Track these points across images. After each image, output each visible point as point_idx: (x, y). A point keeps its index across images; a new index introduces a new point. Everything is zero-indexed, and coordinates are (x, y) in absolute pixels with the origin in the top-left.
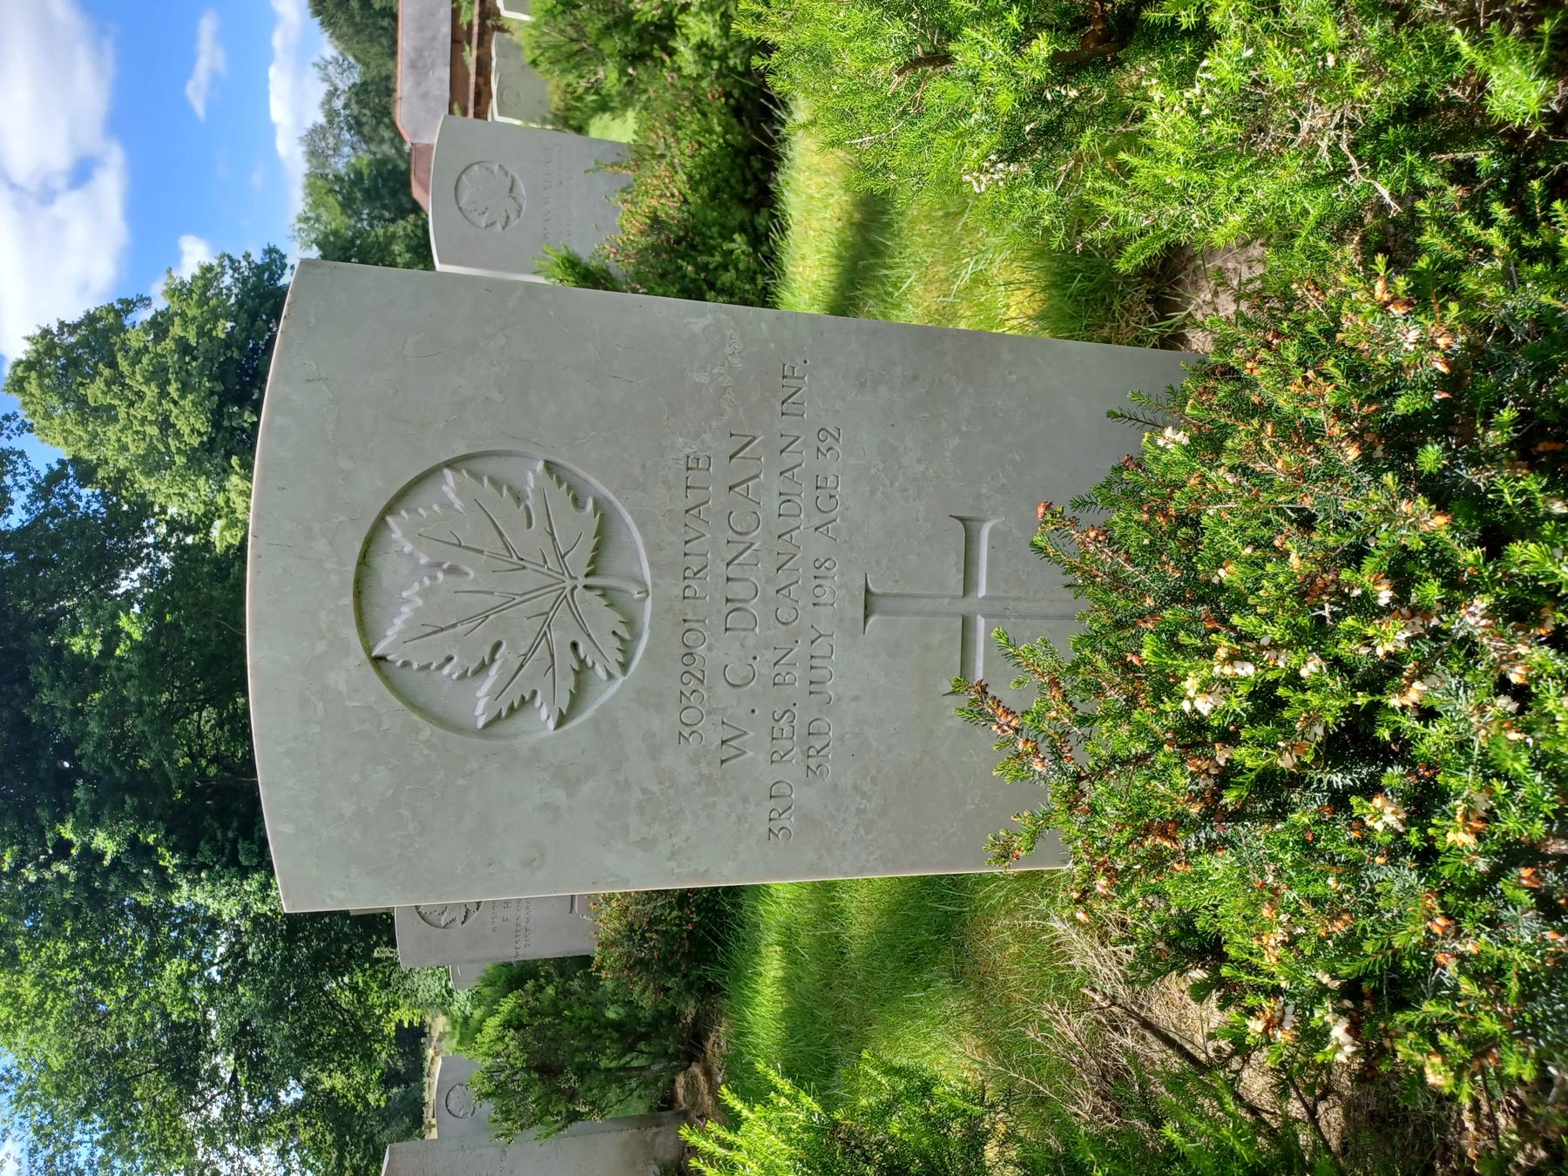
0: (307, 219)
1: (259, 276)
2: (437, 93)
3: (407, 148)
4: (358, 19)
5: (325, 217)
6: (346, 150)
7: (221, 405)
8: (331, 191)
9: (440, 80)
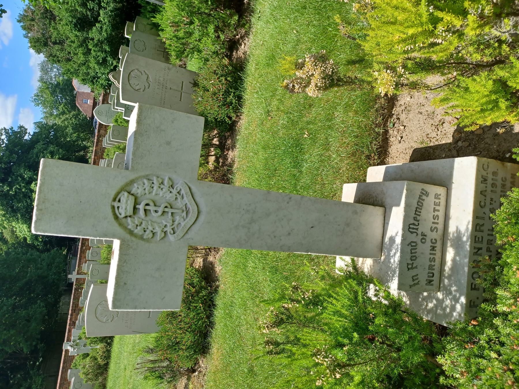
0: (38, 96)
1: (16, 137)
3: (75, 92)
5: (45, 96)
6: (55, 70)
8: (48, 88)
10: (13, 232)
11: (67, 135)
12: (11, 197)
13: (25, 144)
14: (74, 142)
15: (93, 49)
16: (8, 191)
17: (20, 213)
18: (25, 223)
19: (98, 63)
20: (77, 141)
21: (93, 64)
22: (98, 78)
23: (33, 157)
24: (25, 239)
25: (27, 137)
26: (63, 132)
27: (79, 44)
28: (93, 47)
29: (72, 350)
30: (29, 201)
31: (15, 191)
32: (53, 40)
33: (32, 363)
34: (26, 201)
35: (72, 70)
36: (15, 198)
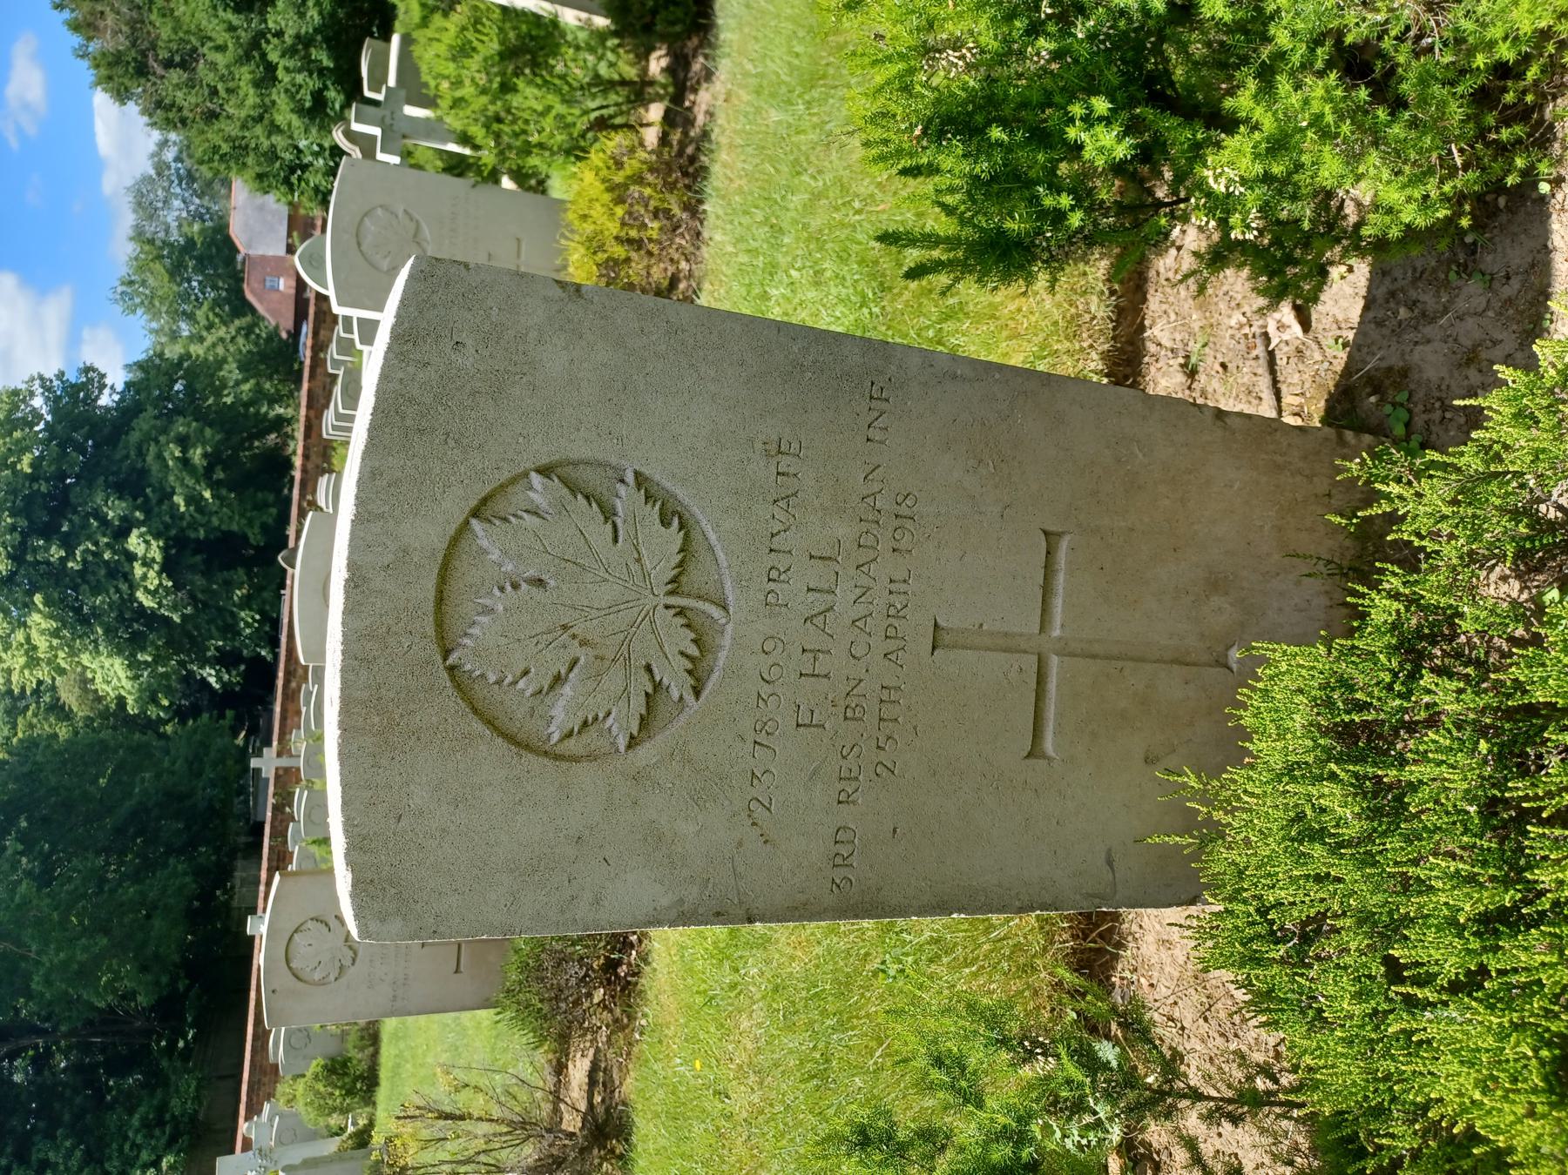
1: (75, 400)
3: (239, 258)
5: (151, 281)
6: (177, 203)
7: (25, 535)
8: (160, 257)
10: (84, 682)
11: (224, 386)
12: (72, 580)
13: (103, 419)
14: (247, 405)
15: (283, 63)
16: (63, 560)
17: (101, 625)
18: (120, 652)
19: (300, 111)
20: (251, 403)
21: (284, 115)
22: (304, 168)
23: (127, 457)
24: (121, 701)
25: (105, 400)
26: (212, 376)
27: (240, 51)
28: (283, 56)
30: (124, 587)
31: (84, 561)
32: (163, 54)
33: (163, 1043)
34: (118, 590)
35: (225, 148)
36: (86, 582)
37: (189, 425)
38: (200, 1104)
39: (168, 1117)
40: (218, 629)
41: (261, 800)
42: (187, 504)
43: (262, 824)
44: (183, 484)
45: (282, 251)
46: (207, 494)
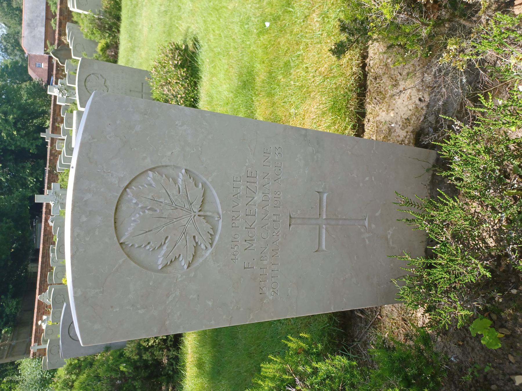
2: (39, 36)
3: (26, 55)
4: (6, 10)
9: (40, 32)
26: (16, 93)
29: (61, 95)
37: (7, 107)
38: (18, 311)
39: (4, 315)
40: (20, 184)
41: (38, 241)
42: (7, 137)
43: (38, 250)
44: (5, 129)
45: (42, 53)
46: (15, 133)
